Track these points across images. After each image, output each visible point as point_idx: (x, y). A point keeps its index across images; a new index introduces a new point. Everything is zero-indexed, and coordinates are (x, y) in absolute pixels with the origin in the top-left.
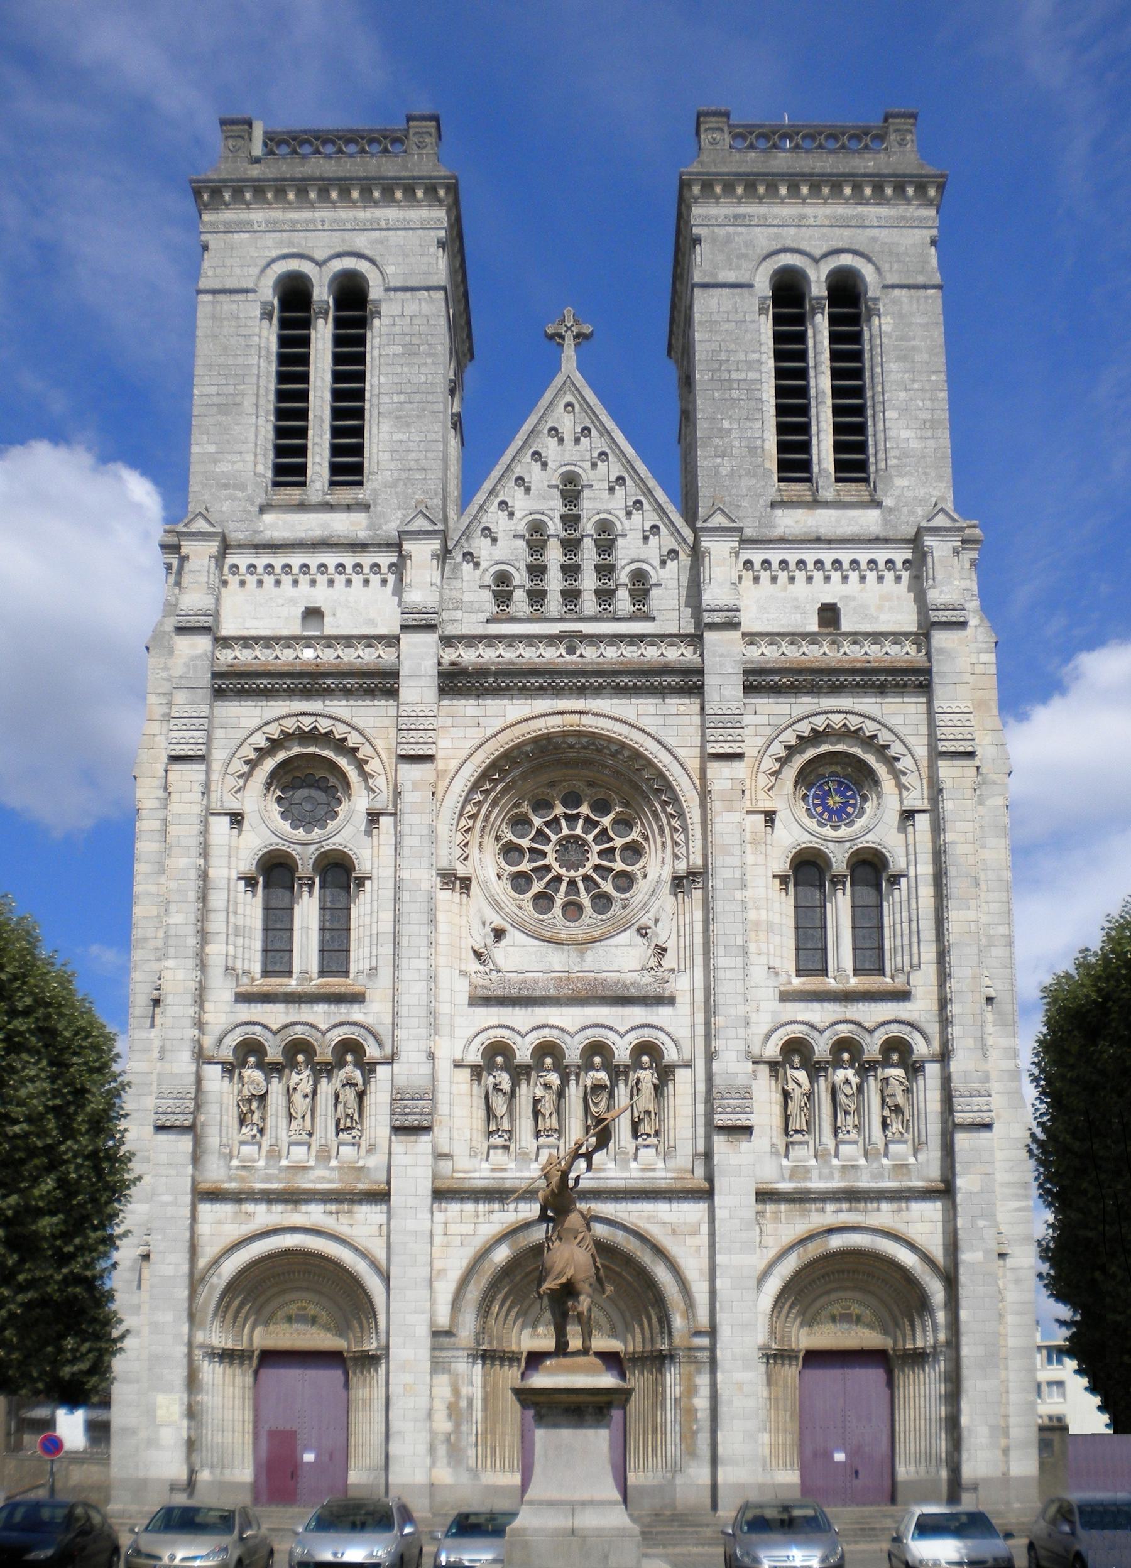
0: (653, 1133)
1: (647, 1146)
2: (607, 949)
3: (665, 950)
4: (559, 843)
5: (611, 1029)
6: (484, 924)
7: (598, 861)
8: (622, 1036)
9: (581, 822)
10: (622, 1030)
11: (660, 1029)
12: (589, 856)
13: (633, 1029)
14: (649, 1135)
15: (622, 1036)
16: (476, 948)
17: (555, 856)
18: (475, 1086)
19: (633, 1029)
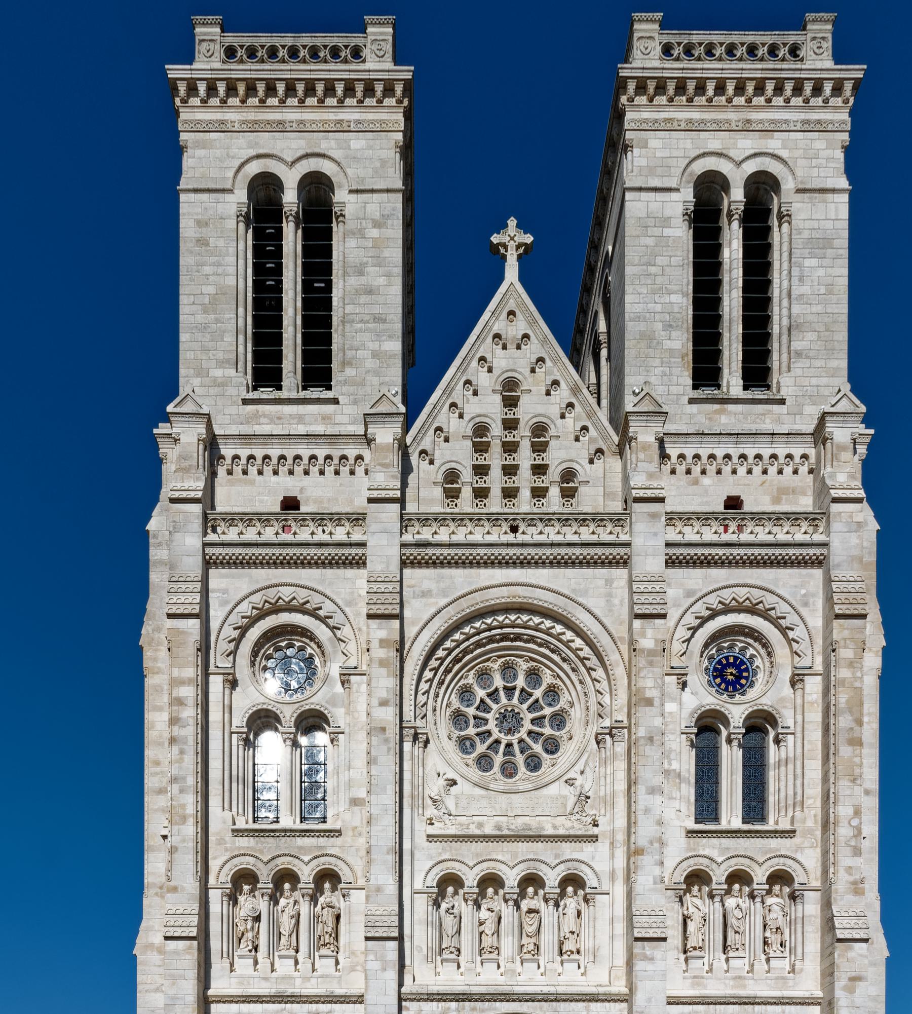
0: (575, 950)
14: (572, 952)
17: (496, 722)
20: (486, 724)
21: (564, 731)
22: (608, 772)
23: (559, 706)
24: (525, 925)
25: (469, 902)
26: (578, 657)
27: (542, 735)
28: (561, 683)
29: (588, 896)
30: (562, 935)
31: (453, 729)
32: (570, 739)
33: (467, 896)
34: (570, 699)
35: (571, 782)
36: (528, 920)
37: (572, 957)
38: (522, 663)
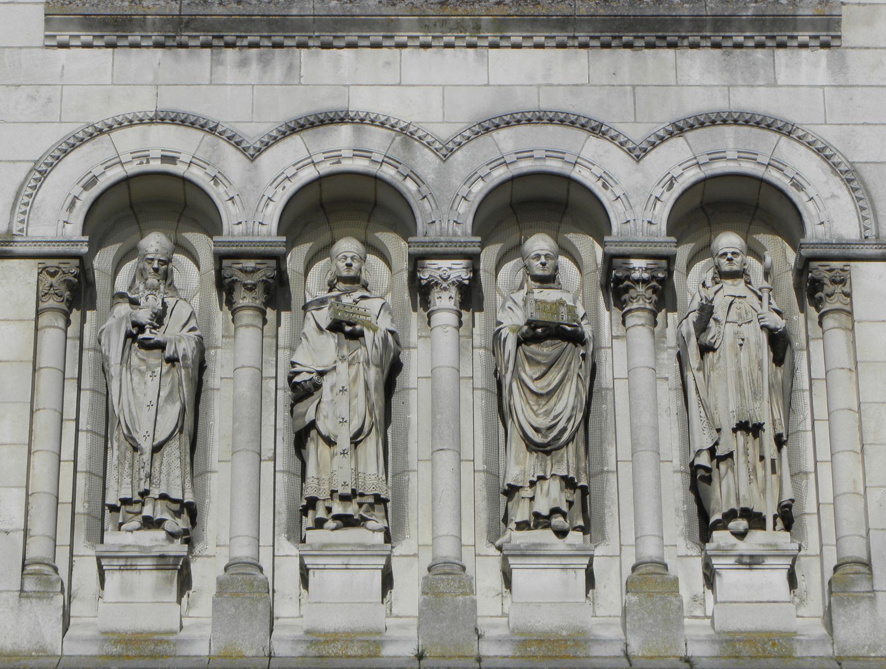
0: (769, 511)
1: (752, 562)
5: (597, 130)
8: (638, 153)
10: (637, 133)
11: (785, 130)
13: (679, 129)
14: (756, 520)
15: (638, 153)
18: (51, 338)
19: (679, 129)
24: (518, 401)
25: (243, 299)
29: (819, 270)
30: (703, 439)
33: (232, 268)
36: (529, 372)
37: (756, 541)
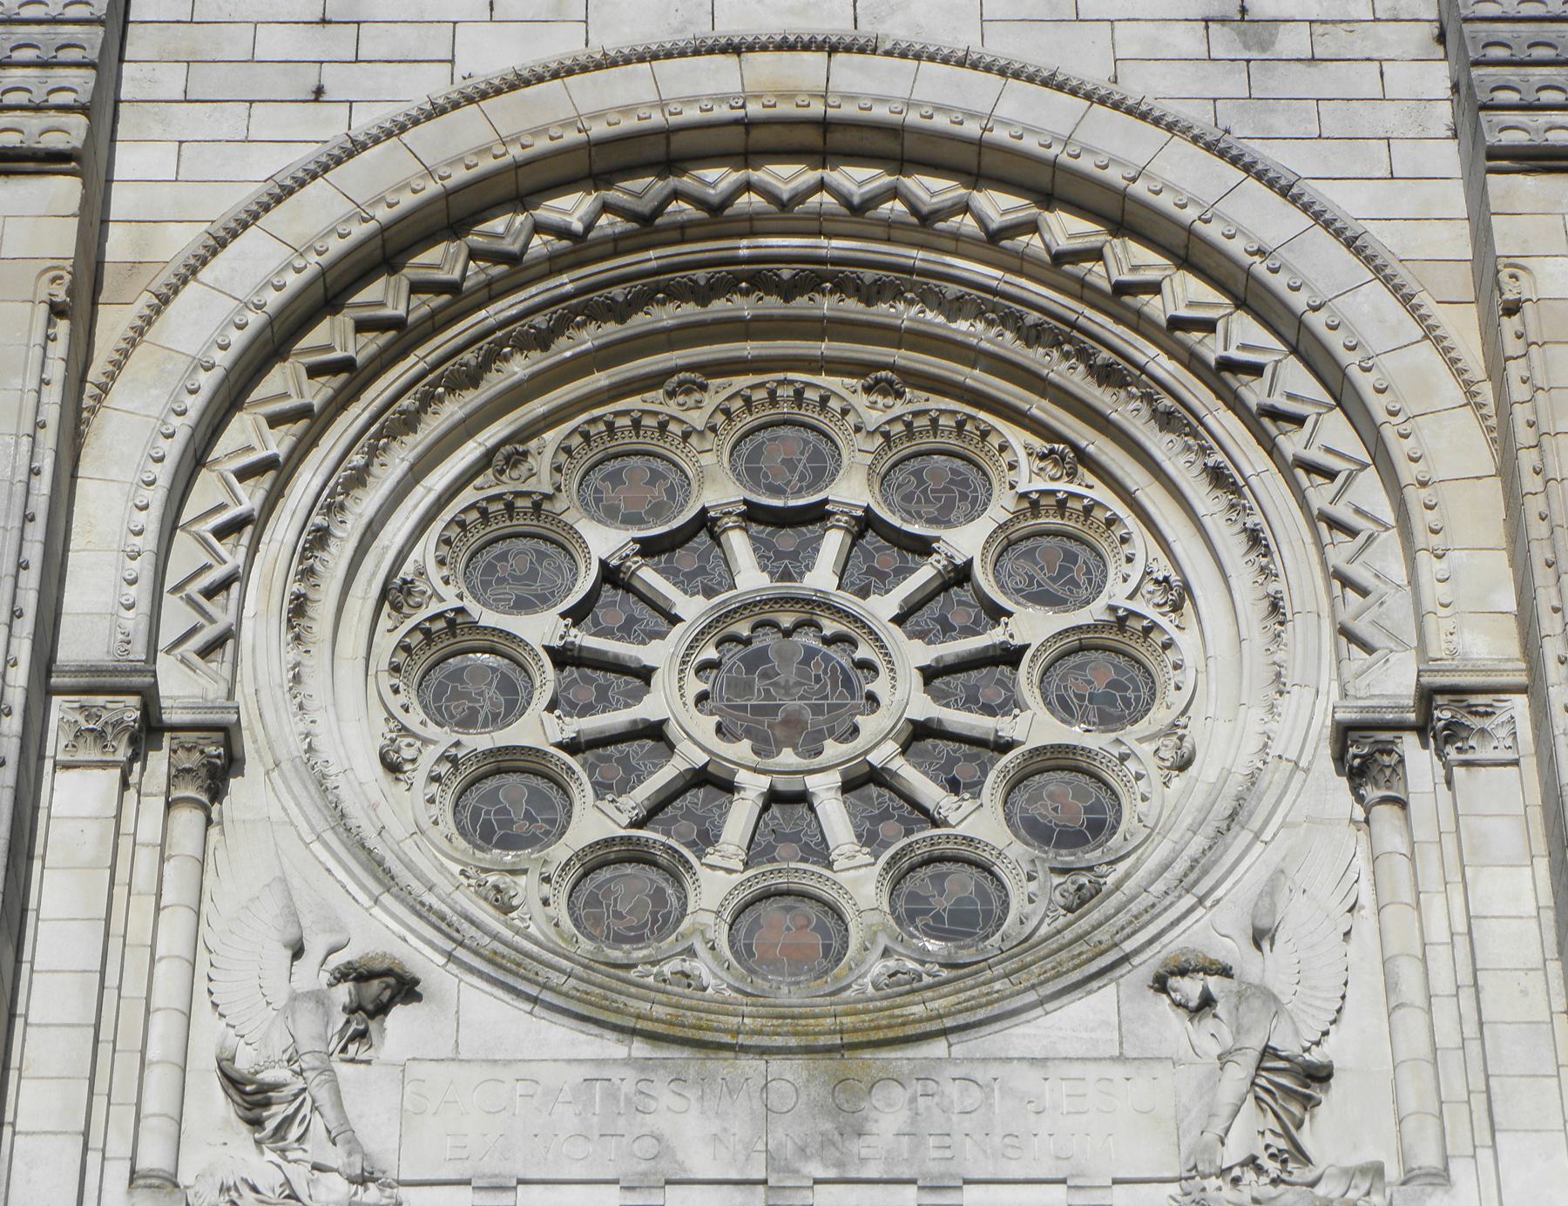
2: (981, 1074)
3: (1319, 1075)
4: (717, 627)
6: (298, 952)
7: (923, 707)
9: (833, 542)
12: (880, 686)
16: (243, 1065)
17: (695, 686)
20: (636, 697)
21: (1142, 727)
22: (1438, 930)
23: (1101, 602)
26: (1193, 362)
27: (1004, 746)
28: (1101, 493)
31: (415, 719)
32: (1183, 765)
34: (1163, 568)
35: (1190, 988)
38: (861, 401)
